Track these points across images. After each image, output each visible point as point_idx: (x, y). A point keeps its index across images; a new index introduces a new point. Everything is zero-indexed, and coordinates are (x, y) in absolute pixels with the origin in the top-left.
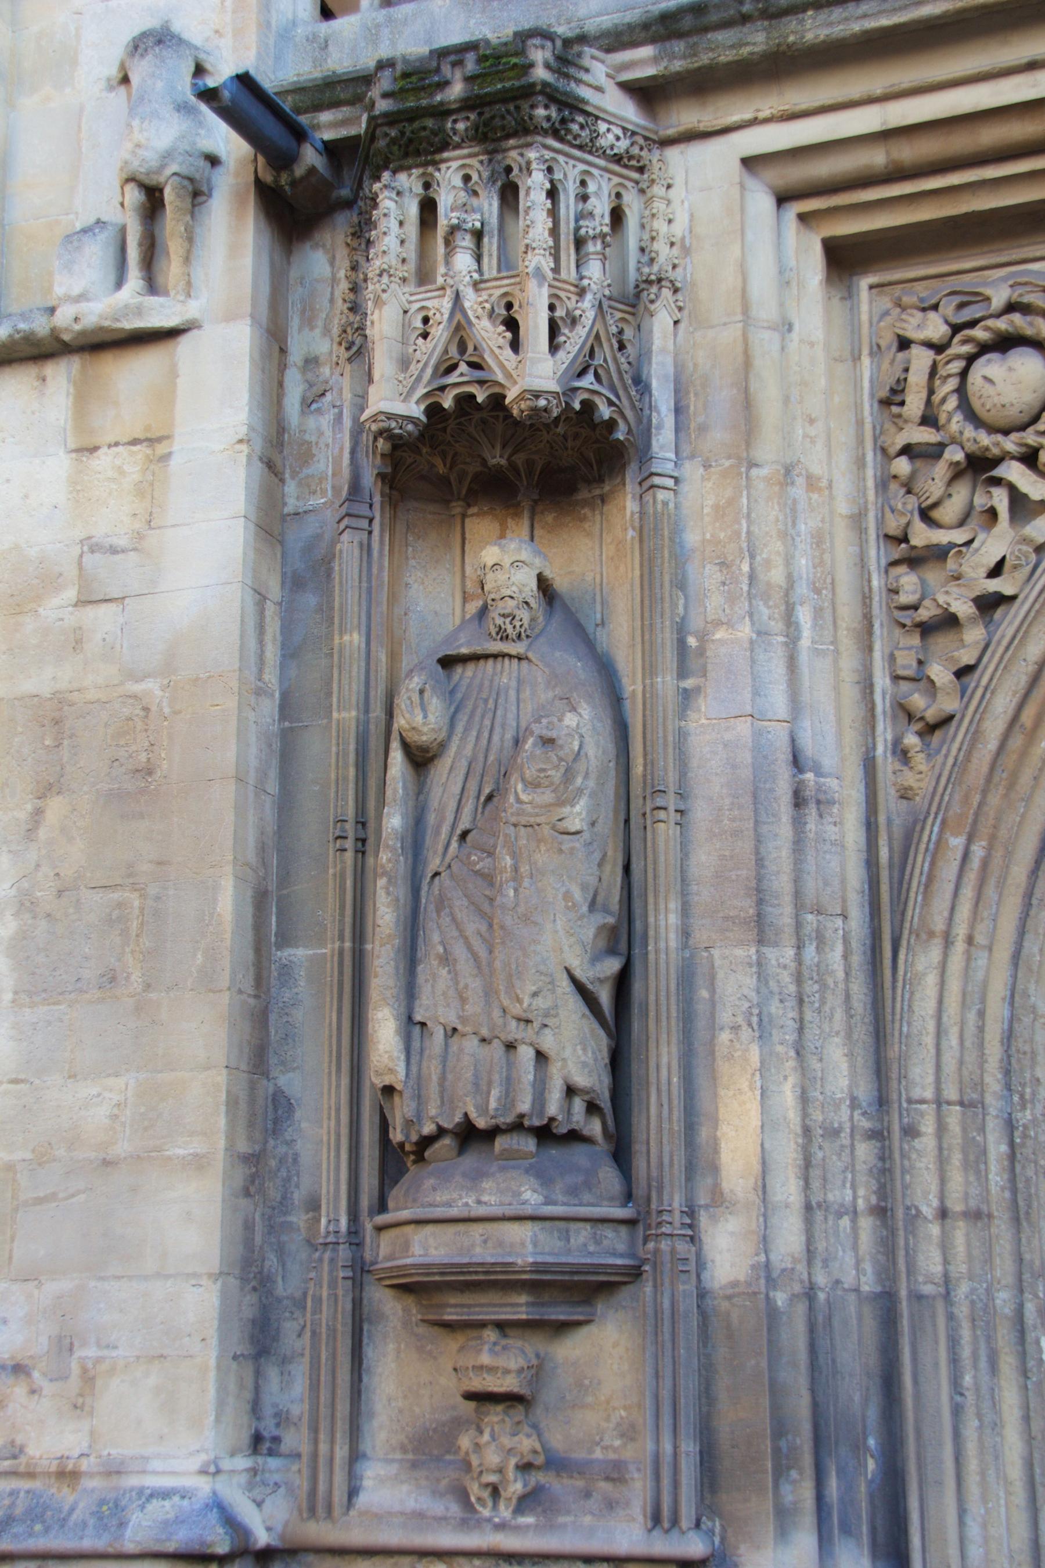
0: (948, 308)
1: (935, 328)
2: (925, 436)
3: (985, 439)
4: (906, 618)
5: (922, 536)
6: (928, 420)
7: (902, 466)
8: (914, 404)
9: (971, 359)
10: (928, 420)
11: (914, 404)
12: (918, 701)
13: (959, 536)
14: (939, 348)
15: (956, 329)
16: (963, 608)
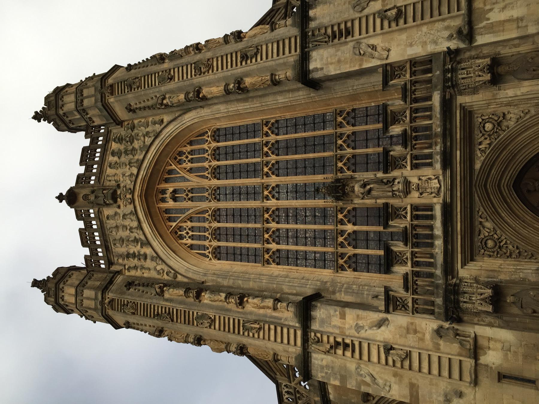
0: (480, 249)
1: (483, 251)
2: (496, 253)
3: (497, 247)
4: (518, 257)
5: (508, 254)
6: (494, 252)
7: (499, 256)
8: (492, 254)
9: (487, 247)
10: (494, 252)
11: (492, 254)
12: (529, 256)
13: (509, 251)
14: (485, 250)
15: (483, 248)
16: (518, 251)
